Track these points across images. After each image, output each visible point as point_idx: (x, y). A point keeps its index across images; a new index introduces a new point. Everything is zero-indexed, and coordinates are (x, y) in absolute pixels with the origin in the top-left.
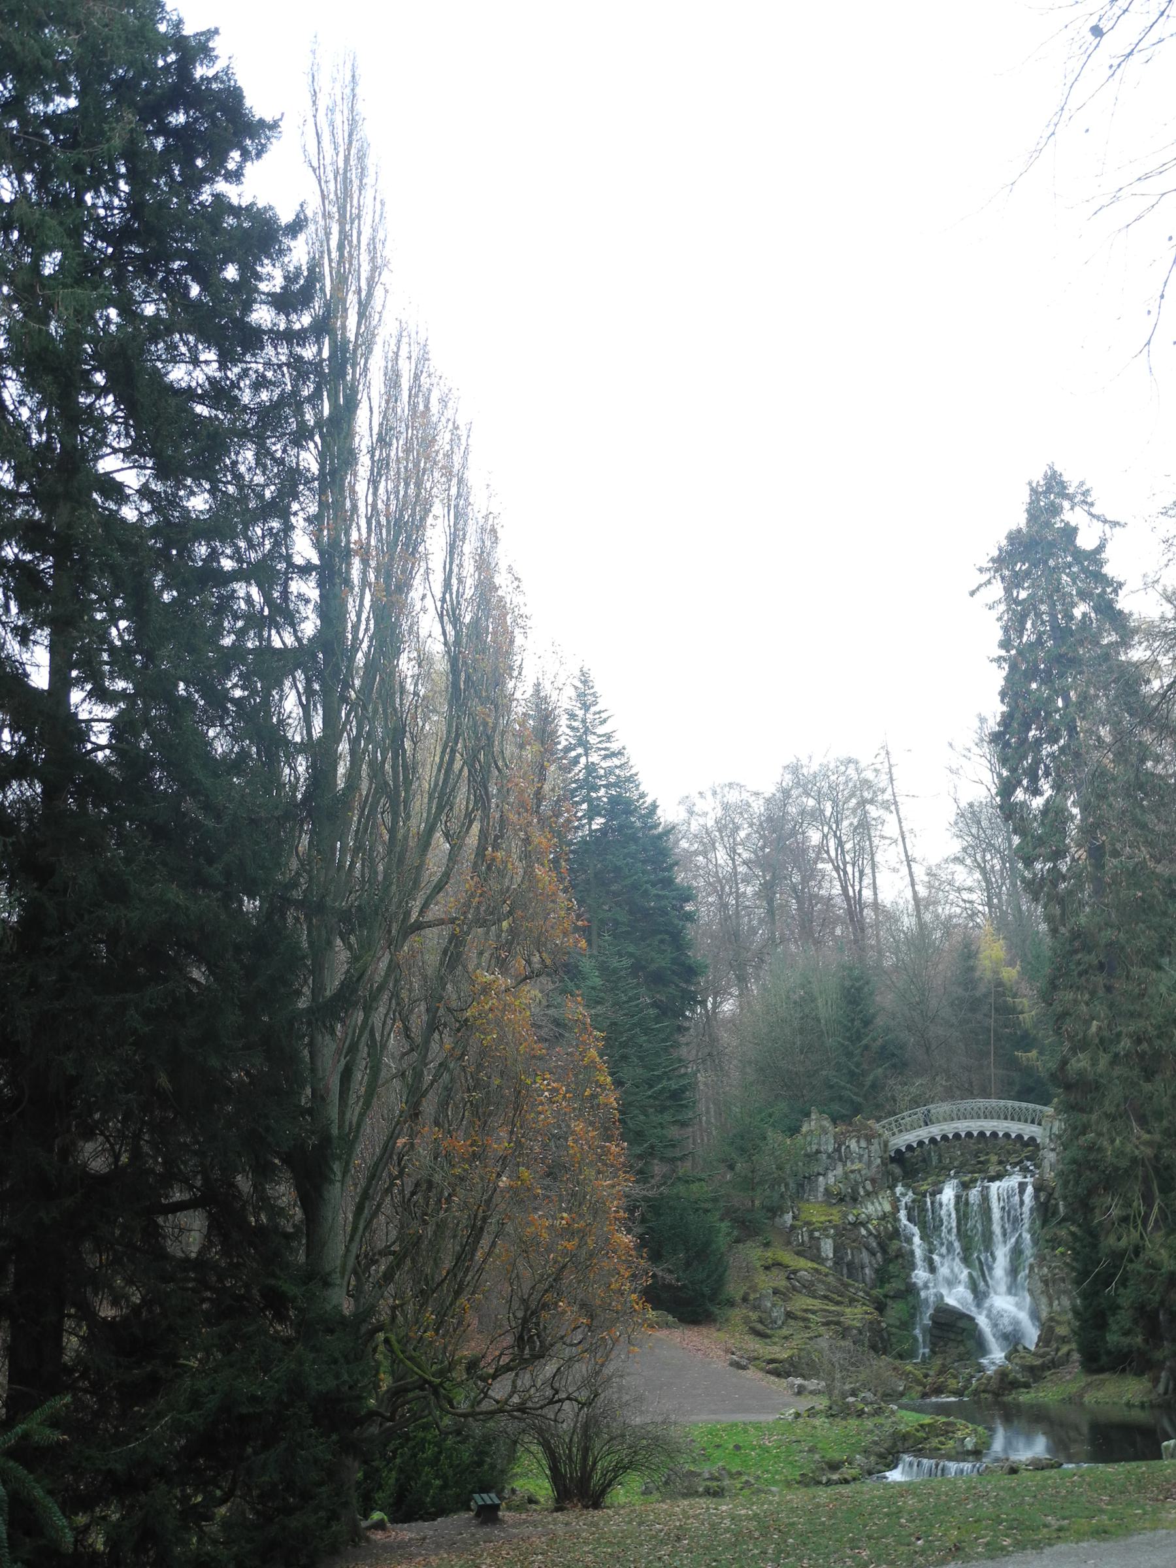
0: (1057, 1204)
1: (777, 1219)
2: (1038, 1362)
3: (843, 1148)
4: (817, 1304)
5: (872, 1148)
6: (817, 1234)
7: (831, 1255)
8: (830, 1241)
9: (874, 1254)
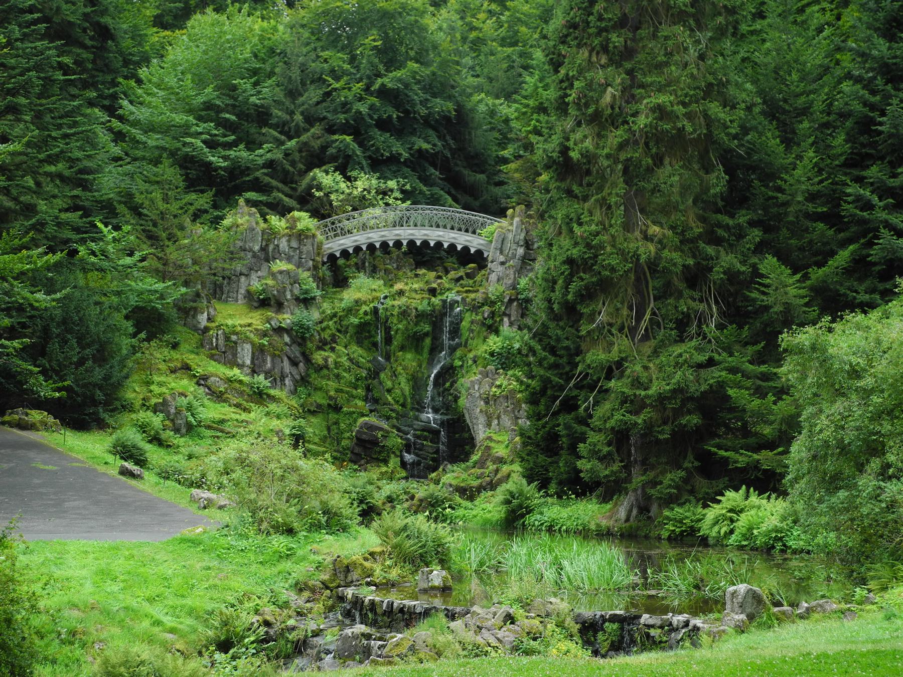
2: (475, 483)
5: (304, 249)
6: (234, 338)
7: (248, 362)
8: (248, 347)
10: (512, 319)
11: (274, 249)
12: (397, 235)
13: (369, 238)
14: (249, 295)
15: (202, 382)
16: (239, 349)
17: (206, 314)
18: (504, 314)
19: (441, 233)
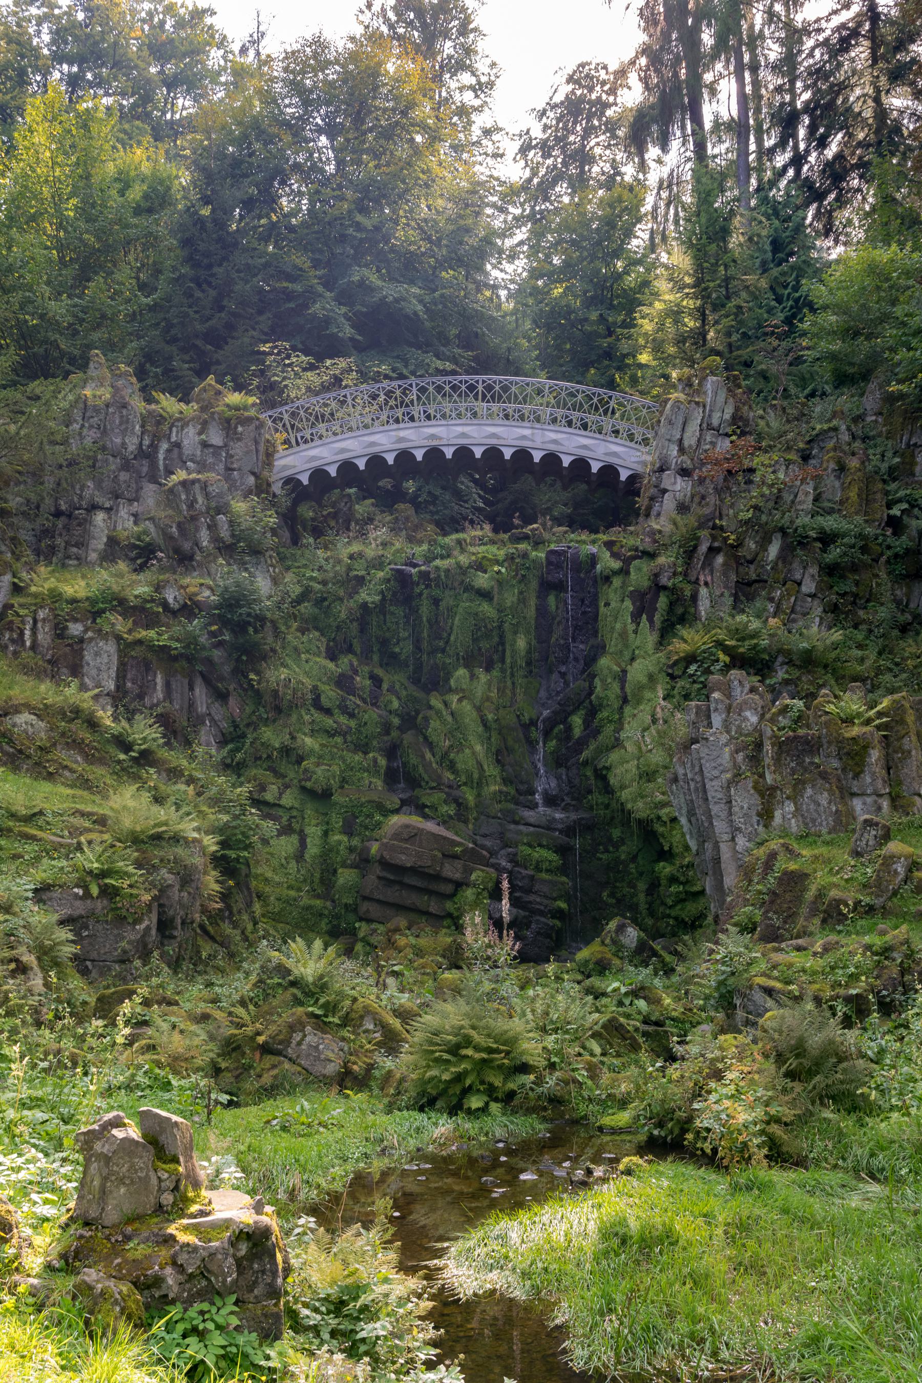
3: (164, 446)
5: (238, 449)
6: (75, 629)
9: (222, 697)
11: (169, 451)
12: (433, 437)
13: (373, 444)
16: (88, 656)
19: (527, 432)
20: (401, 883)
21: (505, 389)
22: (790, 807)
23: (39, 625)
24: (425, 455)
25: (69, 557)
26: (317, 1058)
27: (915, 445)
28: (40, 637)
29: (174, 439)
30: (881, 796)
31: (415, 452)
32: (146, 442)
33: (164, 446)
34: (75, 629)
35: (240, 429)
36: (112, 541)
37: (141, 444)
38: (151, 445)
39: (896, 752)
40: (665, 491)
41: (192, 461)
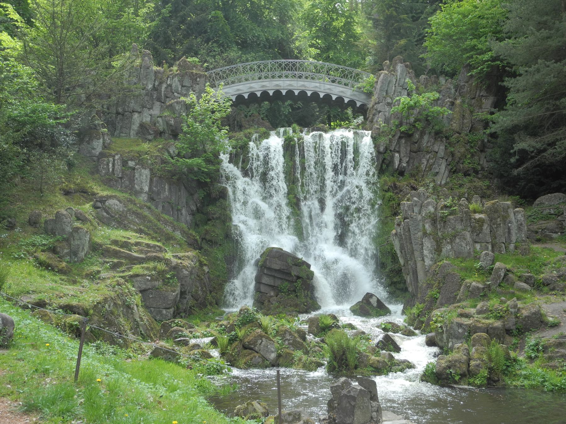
0: (393, 157)
1: (84, 146)
3: (164, 86)
4: (132, 236)
6: (131, 164)
7: (146, 189)
8: (146, 173)
10: (402, 155)
12: (277, 85)
13: (251, 88)
14: (142, 126)
15: (99, 204)
16: (137, 175)
17: (101, 140)
18: (395, 151)
19: (318, 85)
20: (274, 277)
21: (294, 65)
22: (449, 247)
23: (116, 162)
24: (274, 93)
25: (122, 133)
26: (267, 351)
27: (482, 96)
28: (116, 167)
29: (169, 83)
30: (488, 243)
31: (295, 91)
32: (157, 83)
33: (164, 86)
34: (131, 164)
35: (198, 79)
36: (142, 126)
37: (154, 85)
38: (158, 85)
39: (494, 224)
40: (380, 112)
41: (176, 92)
